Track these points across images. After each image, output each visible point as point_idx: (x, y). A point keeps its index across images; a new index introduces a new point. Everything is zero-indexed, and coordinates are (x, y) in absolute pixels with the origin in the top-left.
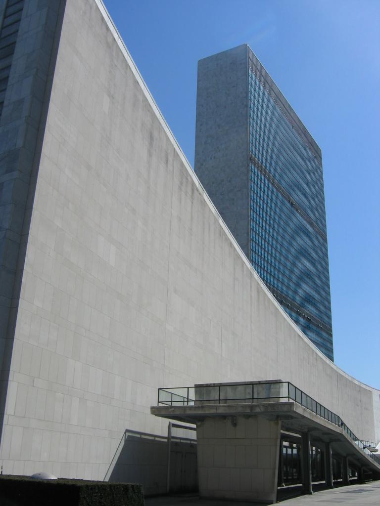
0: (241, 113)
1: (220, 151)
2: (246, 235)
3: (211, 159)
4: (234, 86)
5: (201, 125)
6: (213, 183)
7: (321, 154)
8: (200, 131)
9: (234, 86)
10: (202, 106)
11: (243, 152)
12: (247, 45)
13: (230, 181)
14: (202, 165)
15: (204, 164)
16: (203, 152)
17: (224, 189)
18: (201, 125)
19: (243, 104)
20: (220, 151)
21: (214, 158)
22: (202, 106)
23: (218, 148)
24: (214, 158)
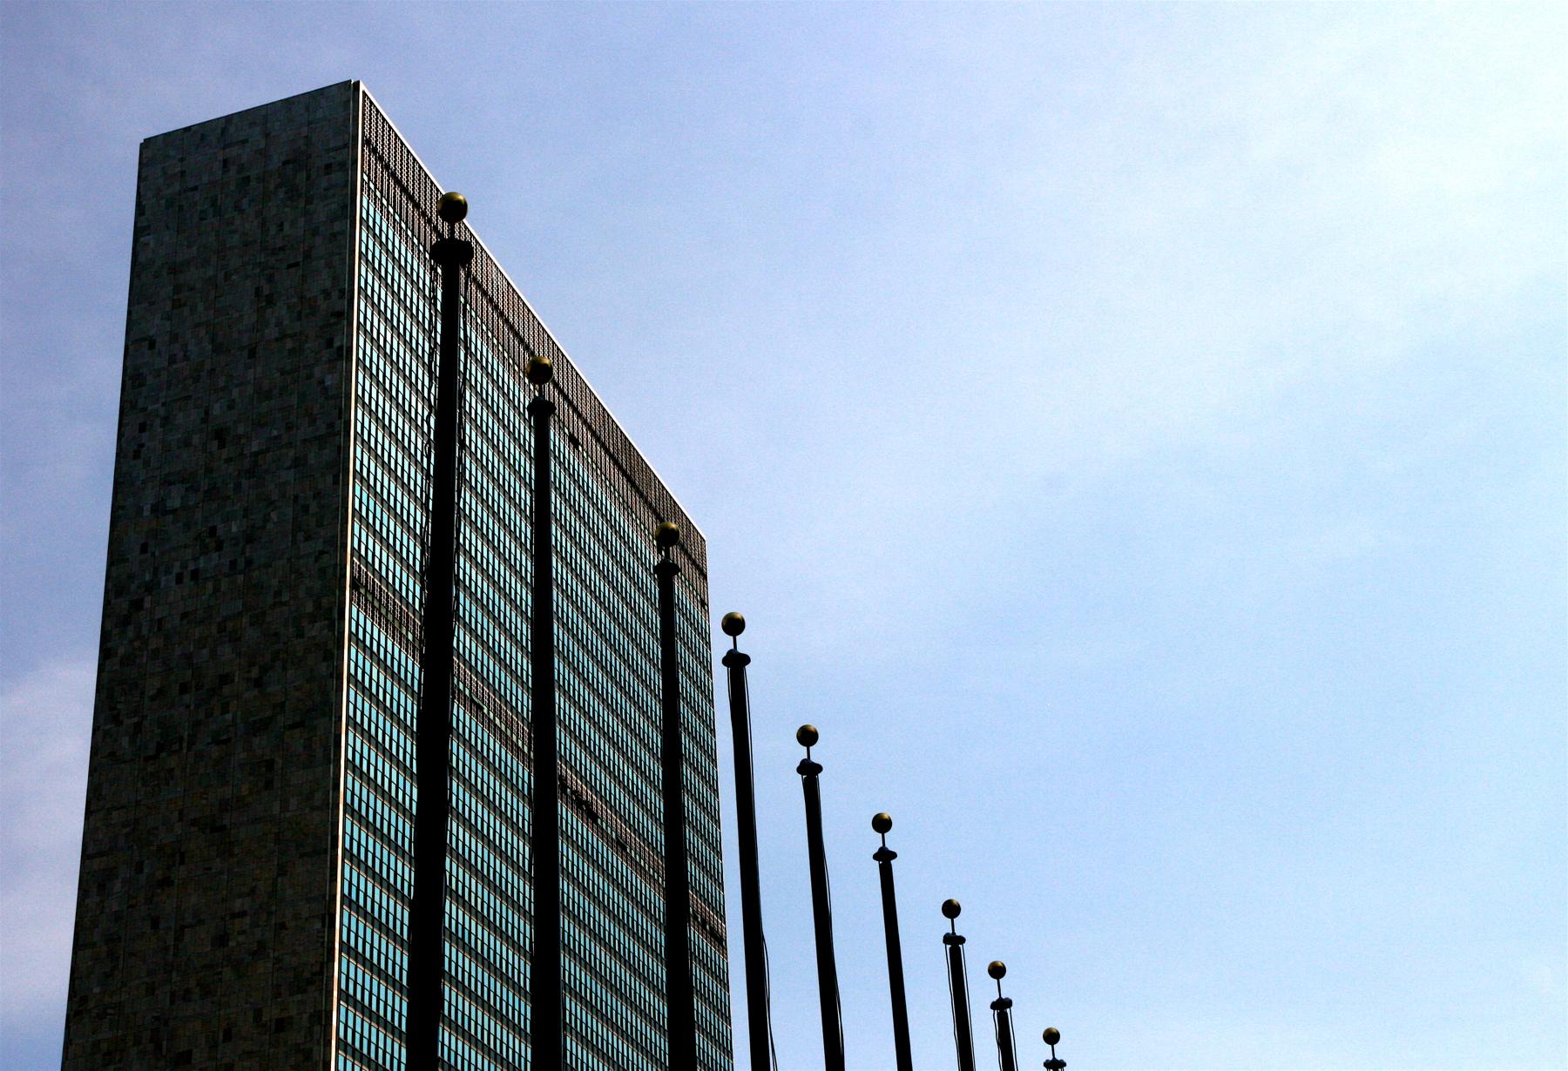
0: (322, 382)
1: (219, 548)
2: (318, 925)
3: (179, 579)
4: (296, 264)
5: (142, 428)
6: (184, 689)
7: (703, 555)
9: (296, 264)
11: (322, 553)
12: (358, 84)
13: (258, 683)
14: (137, 605)
15: (147, 605)
16: (144, 548)
17: (229, 716)
18: (142, 428)
19: (330, 343)
20: (219, 548)
21: (195, 574)
22: (152, 345)
23: (213, 531)
24: (195, 574)
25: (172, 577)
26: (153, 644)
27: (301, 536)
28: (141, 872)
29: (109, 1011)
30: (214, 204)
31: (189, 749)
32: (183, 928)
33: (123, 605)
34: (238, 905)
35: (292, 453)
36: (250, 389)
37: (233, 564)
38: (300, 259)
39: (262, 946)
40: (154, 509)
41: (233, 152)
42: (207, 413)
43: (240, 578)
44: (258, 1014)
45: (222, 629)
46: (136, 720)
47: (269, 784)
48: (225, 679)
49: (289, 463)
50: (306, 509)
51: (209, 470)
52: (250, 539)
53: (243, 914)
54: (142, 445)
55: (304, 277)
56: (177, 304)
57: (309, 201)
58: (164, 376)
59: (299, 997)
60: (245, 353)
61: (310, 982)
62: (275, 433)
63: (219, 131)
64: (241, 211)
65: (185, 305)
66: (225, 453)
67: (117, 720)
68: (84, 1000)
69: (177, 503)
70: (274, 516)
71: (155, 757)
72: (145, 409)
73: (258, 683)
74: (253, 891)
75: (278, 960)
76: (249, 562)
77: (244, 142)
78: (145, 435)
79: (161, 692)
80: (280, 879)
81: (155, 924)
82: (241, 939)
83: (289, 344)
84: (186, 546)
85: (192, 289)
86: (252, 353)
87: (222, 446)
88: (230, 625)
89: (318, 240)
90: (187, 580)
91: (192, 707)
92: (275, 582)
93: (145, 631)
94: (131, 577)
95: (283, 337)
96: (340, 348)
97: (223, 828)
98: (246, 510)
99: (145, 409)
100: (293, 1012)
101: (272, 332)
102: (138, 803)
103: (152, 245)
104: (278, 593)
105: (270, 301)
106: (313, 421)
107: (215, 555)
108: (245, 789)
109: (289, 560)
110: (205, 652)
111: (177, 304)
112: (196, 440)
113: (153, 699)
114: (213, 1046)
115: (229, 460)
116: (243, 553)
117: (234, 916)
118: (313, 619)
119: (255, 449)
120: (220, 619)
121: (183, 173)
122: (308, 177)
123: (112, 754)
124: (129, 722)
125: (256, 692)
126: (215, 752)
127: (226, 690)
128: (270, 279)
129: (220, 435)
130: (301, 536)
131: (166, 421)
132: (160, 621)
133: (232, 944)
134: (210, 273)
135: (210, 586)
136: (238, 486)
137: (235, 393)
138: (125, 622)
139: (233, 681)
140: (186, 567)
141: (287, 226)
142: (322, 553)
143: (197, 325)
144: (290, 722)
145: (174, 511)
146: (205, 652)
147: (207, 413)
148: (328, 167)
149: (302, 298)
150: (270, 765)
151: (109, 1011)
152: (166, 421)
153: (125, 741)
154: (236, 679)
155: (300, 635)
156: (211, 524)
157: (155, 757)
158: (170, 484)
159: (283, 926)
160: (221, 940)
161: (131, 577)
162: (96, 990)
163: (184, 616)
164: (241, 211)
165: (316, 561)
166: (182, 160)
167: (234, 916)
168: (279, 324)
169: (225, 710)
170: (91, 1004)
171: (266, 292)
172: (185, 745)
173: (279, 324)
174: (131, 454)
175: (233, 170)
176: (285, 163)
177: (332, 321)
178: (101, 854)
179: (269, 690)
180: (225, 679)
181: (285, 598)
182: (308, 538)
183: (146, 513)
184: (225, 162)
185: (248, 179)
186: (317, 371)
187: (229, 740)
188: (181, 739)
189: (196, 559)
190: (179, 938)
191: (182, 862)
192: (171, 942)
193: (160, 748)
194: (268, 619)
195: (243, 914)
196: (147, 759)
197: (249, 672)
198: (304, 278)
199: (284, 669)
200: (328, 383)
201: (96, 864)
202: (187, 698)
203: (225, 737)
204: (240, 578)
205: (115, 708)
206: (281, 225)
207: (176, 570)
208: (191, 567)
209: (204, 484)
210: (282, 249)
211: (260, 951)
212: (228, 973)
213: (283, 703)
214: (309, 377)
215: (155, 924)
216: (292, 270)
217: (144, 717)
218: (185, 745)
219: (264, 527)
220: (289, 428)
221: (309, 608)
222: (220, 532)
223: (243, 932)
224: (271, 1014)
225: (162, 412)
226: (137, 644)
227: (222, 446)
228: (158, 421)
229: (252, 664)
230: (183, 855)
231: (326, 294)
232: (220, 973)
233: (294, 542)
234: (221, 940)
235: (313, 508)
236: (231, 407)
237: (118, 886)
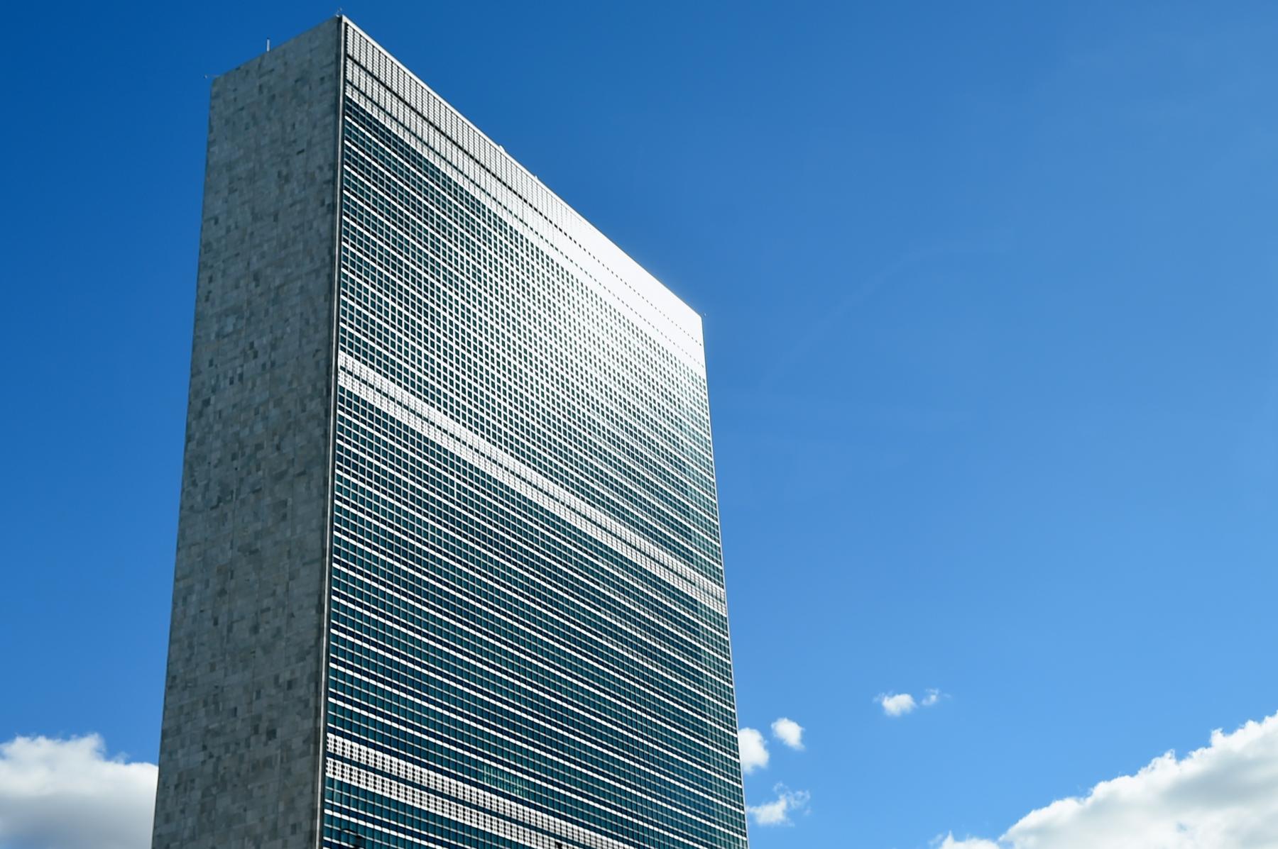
0: (318, 231)
2: (313, 612)
3: (231, 383)
5: (211, 280)
6: (234, 457)
8: (207, 299)
10: (216, 222)
13: (278, 448)
14: (206, 403)
15: (212, 402)
16: (211, 364)
17: (260, 473)
18: (211, 280)
19: (323, 203)
20: (256, 356)
21: (241, 376)
22: (216, 222)
23: (252, 344)
25: (228, 381)
26: (217, 427)
27: (304, 341)
28: (207, 586)
29: (190, 685)
30: (254, 117)
31: (236, 499)
32: (232, 623)
33: (198, 404)
34: (267, 602)
35: (299, 284)
36: (274, 243)
37: (264, 366)
38: (305, 146)
39: (279, 630)
40: (218, 336)
41: (265, 78)
42: (248, 264)
43: (268, 376)
44: (277, 678)
45: (257, 413)
46: (205, 482)
47: (284, 517)
48: (259, 447)
49: (297, 291)
50: (307, 322)
51: (249, 303)
52: (274, 347)
53: (268, 609)
55: (308, 158)
56: (232, 191)
57: (310, 106)
58: (223, 242)
60: (272, 218)
61: (308, 653)
62: (289, 271)
63: (257, 66)
64: (269, 119)
65: (236, 190)
66: (259, 290)
67: (194, 484)
68: (174, 678)
69: (230, 329)
70: (288, 330)
71: (217, 506)
72: (212, 267)
73: (278, 448)
74: (274, 594)
75: (288, 639)
76: (273, 364)
77: (273, 70)
78: (212, 285)
79: (220, 461)
80: (290, 583)
81: (216, 623)
82: (267, 627)
83: (298, 207)
84: (235, 358)
85: (240, 179)
86: (276, 219)
87: (257, 286)
88: (261, 409)
89: (316, 132)
90: (236, 381)
91: (239, 469)
92: (289, 376)
93: (211, 419)
96: (329, 205)
97: (257, 551)
98: (271, 327)
99: (212, 267)
100: (298, 674)
101: (288, 201)
102: (206, 539)
103: (217, 152)
104: (291, 383)
105: (287, 179)
106: (312, 260)
107: (253, 362)
108: (270, 524)
109: (297, 358)
110: (247, 430)
111: (232, 191)
112: (242, 283)
113: (216, 466)
114: (251, 703)
115: (261, 295)
116: (270, 357)
117: (263, 611)
118: (312, 399)
119: (277, 282)
120: (255, 406)
121: (235, 99)
122: (310, 88)
123: (192, 507)
124: (201, 484)
125: (276, 454)
126: (252, 498)
127: (259, 455)
128: (287, 163)
129: (256, 278)
130: (304, 341)
131: (224, 272)
132: (220, 412)
133: (261, 630)
134: (251, 165)
135: (250, 385)
136: (267, 312)
137: (266, 247)
138: (200, 414)
139: (263, 448)
140: (236, 372)
141: (297, 126)
143: (243, 204)
144: (298, 472)
145: (228, 335)
146: (247, 430)
147: (248, 264)
148: (322, 79)
149: (306, 173)
150: (285, 503)
151: (190, 685)
152: (224, 272)
153: (199, 498)
154: (265, 446)
155: (304, 411)
156: (251, 340)
157: (217, 506)
158: (227, 316)
159: (292, 615)
160: (255, 629)
162: (181, 671)
163: (234, 406)
164: (269, 119)
165: (314, 356)
166: (235, 90)
167: (263, 611)
168: (292, 194)
169: (258, 470)
170: (178, 681)
171: (284, 173)
172: (234, 496)
173: (292, 194)
174: (204, 299)
175: (265, 91)
176: (296, 81)
177: (325, 186)
178: (184, 577)
179: (284, 451)
181: (295, 385)
182: (309, 342)
183: (213, 337)
184: (261, 87)
185: (273, 97)
186: (315, 225)
187: (260, 489)
188: (232, 492)
189: (242, 366)
190: (230, 629)
191: (232, 578)
192: (225, 633)
193: (220, 500)
194: (285, 402)
195: (268, 609)
196: (212, 508)
197: (273, 440)
198: (308, 158)
199: (295, 435)
201: (181, 585)
202: (235, 463)
203: (258, 487)
205: (192, 476)
206: (294, 125)
207: (230, 374)
208: (239, 371)
209: (247, 314)
210: (295, 141)
211: (278, 633)
212: (259, 653)
213: (293, 459)
214: (311, 228)
215: (216, 623)
216: (301, 156)
217: (210, 480)
218: (234, 496)
219: (282, 338)
220: (297, 266)
221: (309, 390)
222: (256, 345)
223: (268, 623)
224: (285, 676)
225: (222, 266)
226: (206, 430)
227: (257, 286)
228: (219, 275)
229: (274, 434)
230: (232, 572)
231: (321, 168)
232: (254, 652)
233: (300, 346)
234: (255, 629)
235: (312, 321)
236: (263, 256)
237: (194, 598)
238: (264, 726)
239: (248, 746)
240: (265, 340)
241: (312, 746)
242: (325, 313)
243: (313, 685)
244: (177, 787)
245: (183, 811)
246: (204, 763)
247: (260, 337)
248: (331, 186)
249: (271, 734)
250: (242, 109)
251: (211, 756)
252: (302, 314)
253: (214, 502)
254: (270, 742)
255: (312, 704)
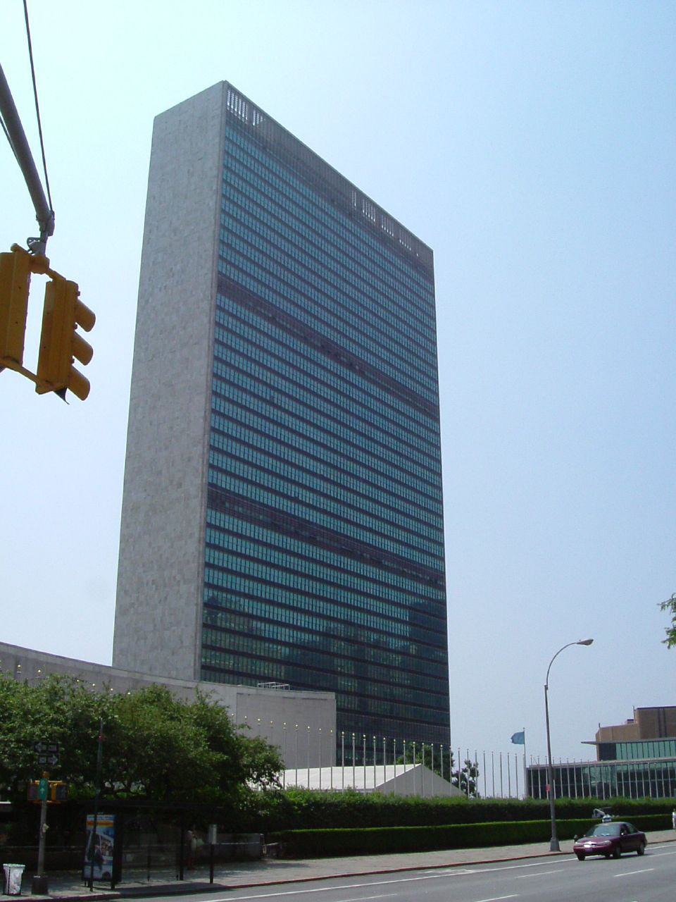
0: (209, 204)
3: (160, 290)
8: (148, 243)
10: (154, 198)
11: (206, 274)
13: (184, 328)
14: (147, 301)
15: (150, 301)
17: (175, 342)
21: (165, 287)
22: (154, 198)
37: (177, 282)
42: (171, 223)
46: (146, 346)
48: (174, 327)
51: (170, 245)
54: (150, 239)
59: (195, 448)
62: (193, 227)
70: (191, 261)
71: (152, 359)
73: (184, 328)
75: (188, 435)
83: (198, 191)
94: (146, 290)
95: (195, 189)
97: (172, 385)
104: (192, 291)
107: (172, 279)
113: (152, 337)
119: (186, 235)
130: (200, 267)
133: (174, 429)
135: (170, 291)
142: (206, 274)
147: (171, 223)
148: (213, 117)
150: (188, 359)
153: (143, 354)
155: (199, 308)
160: (171, 428)
161: (146, 290)
163: (162, 304)
170: (132, 454)
180: (174, 327)
181: (194, 293)
183: (151, 264)
185: (187, 126)
187: (175, 351)
193: (154, 356)
195: (178, 418)
199: (193, 321)
200: (211, 204)
204: (179, 287)
227: (175, 235)
231: (211, 169)
238: (175, 483)
239: (168, 491)
240: (178, 267)
241: (200, 493)
242: (212, 252)
243: (201, 460)
244: (132, 509)
245: (135, 523)
246: (145, 498)
247: (175, 265)
248: (216, 179)
249: (180, 485)
250: (170, 133)
251: (149, 495)
252: (199, 253)
253: (150, 358)
254: (179, 490)
255: (200, 471)
